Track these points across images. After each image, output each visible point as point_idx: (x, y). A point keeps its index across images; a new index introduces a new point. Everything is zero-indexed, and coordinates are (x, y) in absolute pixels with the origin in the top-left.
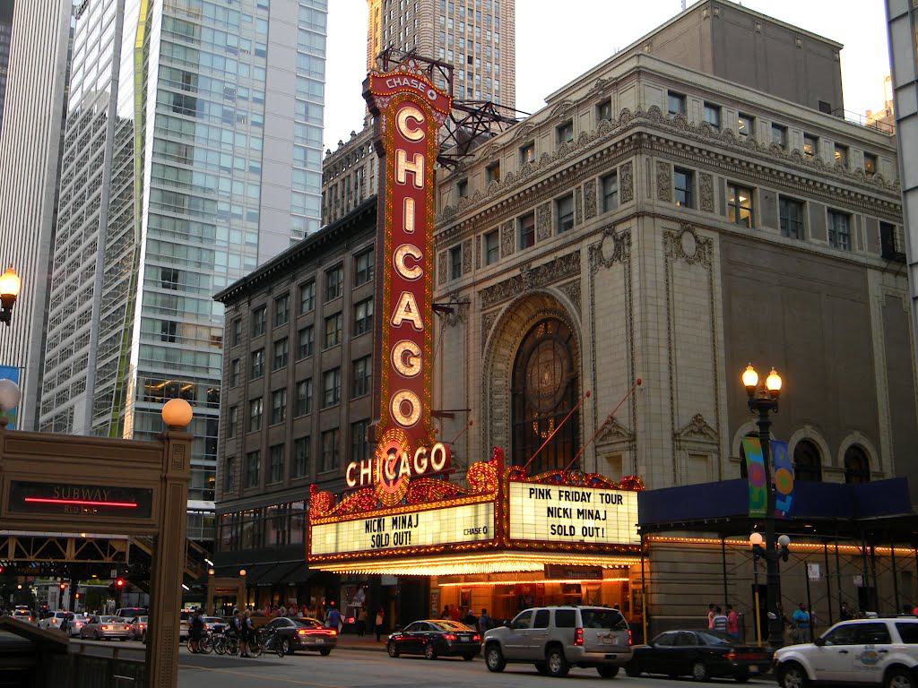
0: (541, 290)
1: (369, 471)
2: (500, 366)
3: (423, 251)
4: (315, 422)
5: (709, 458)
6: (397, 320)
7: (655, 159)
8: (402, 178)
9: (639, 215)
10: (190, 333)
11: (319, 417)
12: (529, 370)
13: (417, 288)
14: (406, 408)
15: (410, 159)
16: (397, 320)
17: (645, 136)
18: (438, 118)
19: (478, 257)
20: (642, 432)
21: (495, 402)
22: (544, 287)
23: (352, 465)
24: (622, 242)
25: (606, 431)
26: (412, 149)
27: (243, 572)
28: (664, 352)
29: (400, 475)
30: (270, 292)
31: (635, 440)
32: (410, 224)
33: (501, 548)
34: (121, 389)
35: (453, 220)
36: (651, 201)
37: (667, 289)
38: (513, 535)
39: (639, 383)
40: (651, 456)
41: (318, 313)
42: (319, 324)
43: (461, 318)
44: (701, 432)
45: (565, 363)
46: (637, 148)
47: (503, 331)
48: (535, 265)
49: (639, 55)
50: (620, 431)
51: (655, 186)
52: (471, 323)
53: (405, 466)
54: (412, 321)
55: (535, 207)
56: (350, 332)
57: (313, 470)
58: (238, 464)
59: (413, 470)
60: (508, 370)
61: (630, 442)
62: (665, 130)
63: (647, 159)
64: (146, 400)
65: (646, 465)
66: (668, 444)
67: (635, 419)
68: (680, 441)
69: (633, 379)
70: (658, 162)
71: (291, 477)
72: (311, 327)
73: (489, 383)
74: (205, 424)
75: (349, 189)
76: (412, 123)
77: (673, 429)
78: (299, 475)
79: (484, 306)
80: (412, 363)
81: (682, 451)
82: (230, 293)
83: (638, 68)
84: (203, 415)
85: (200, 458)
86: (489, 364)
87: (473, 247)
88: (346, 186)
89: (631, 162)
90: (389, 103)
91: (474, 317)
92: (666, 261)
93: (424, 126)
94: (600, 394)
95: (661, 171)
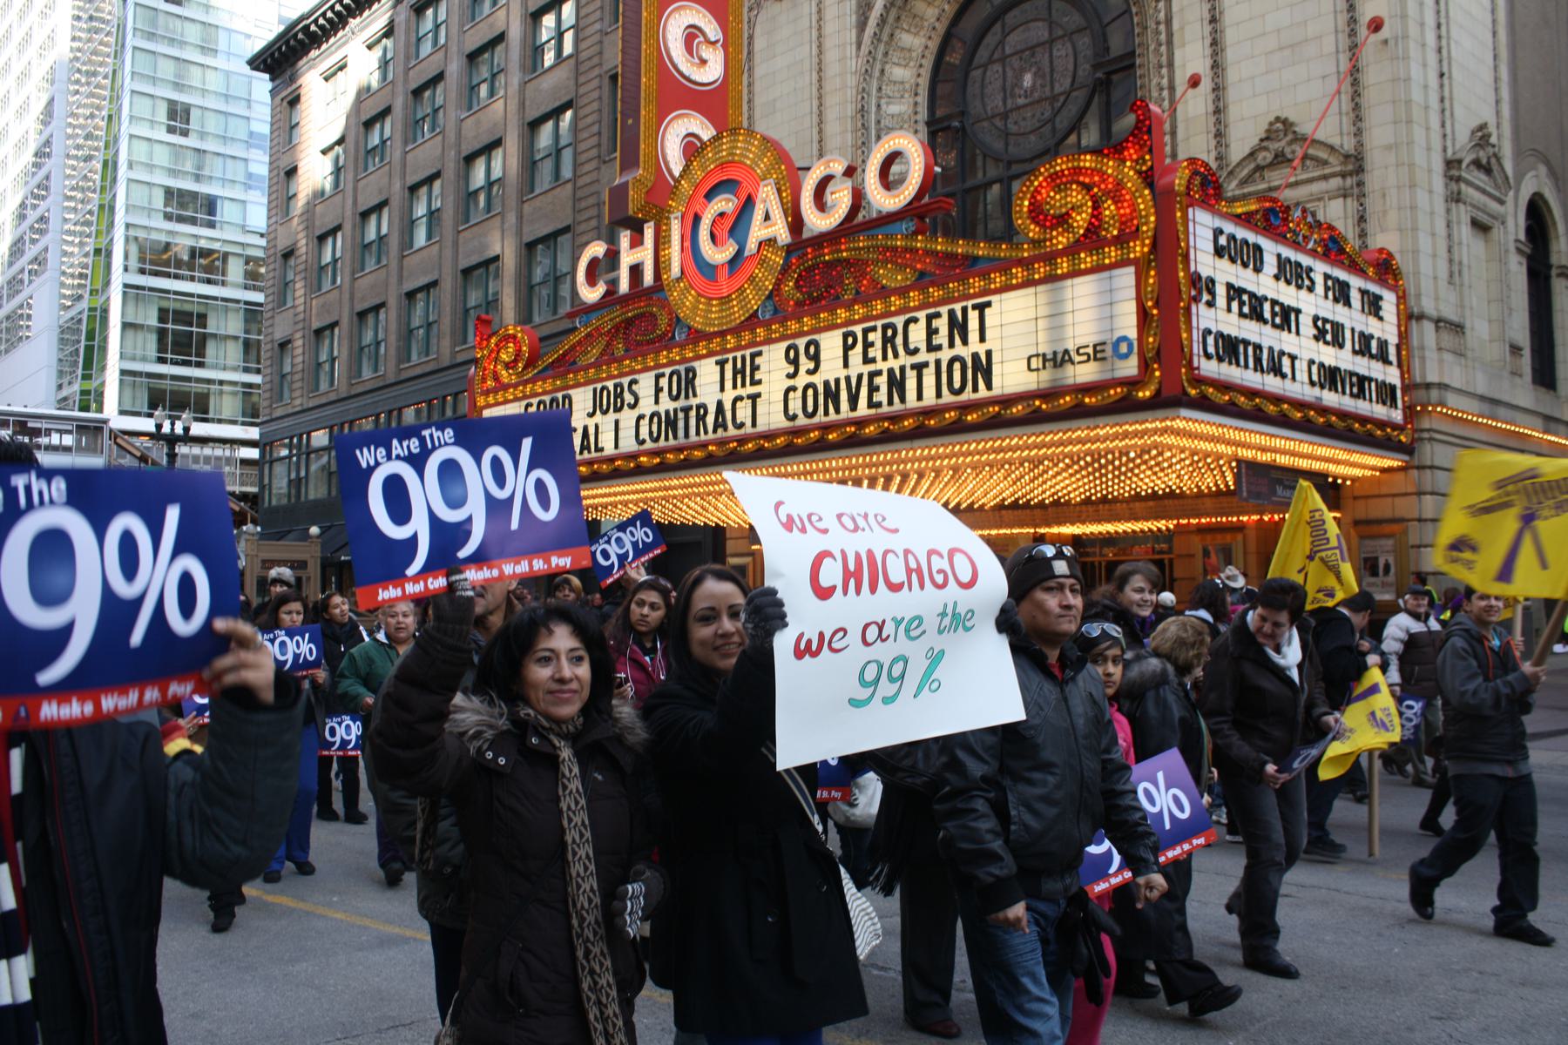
1: (645, 255)
2: (898, 73)
4: (448, 253)
5: (1495, 231)
10: (213, 124)
11: (456, 244)
12: (976, 74)
20: (1389, 148)
23: (597, 249)
25: (1265, 157)
27: (314, 530)
29: (751, 246)
31: (1360, 170)
33: (1166, 401)
39: (1376, 25)
41: (454, 48)
42: (454, 68)
44: (1488, 170)
45: (1084, 41)
50: (1311, 151)
53: (767, 217)
56: (523, 68)
57: (446, 343)
58: (300, 351)
59: (796, 224)
60: (920, 80)
61: (1343, 175)
64: (142, 272)
65: (1400, 230)
66: (1438, 182)
67: (1359, 118)
68: (1459, 179)
69: (1353, 21)
71: (400, 361)
72: (439, 77)
73: (874, 109)
74: (242, 313)
77: (1445, 150)
78: (414, 357)
80: (705, 55)
81: (1462, 206)
82: (287, 42)
84: (238, 301)
85: (235, 369)
86: (872, 71)
94: (1232, 75)
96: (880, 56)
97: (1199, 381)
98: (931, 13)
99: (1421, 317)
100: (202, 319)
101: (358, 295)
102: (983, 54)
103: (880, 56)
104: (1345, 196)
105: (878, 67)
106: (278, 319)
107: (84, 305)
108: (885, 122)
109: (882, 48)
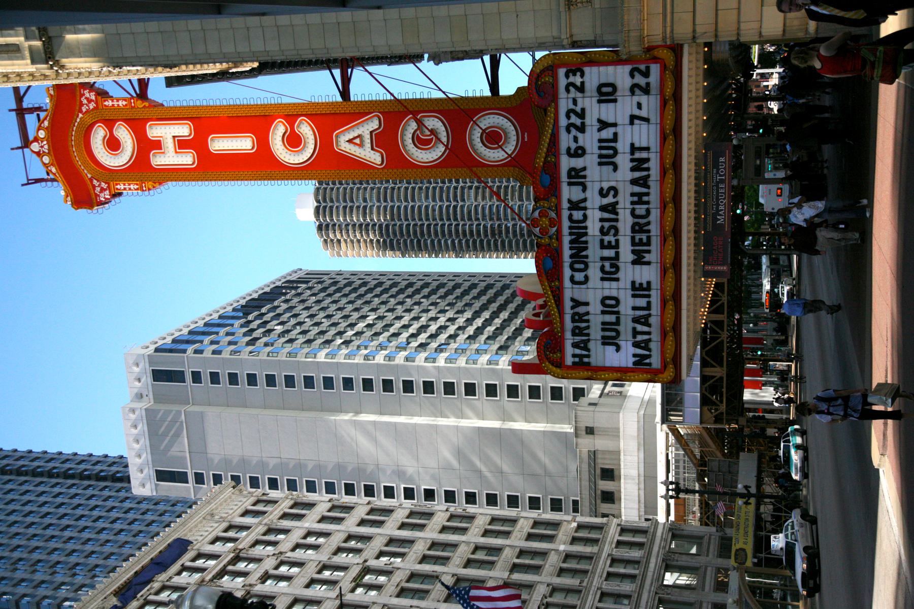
6: (375, 158)
8: (187, 159)
16: (375, 158)
18: (89, 101)
32: (243, 144)
54: (371, 132)
76: (113, 145)
93: (110, 124)
97: (665, 366)
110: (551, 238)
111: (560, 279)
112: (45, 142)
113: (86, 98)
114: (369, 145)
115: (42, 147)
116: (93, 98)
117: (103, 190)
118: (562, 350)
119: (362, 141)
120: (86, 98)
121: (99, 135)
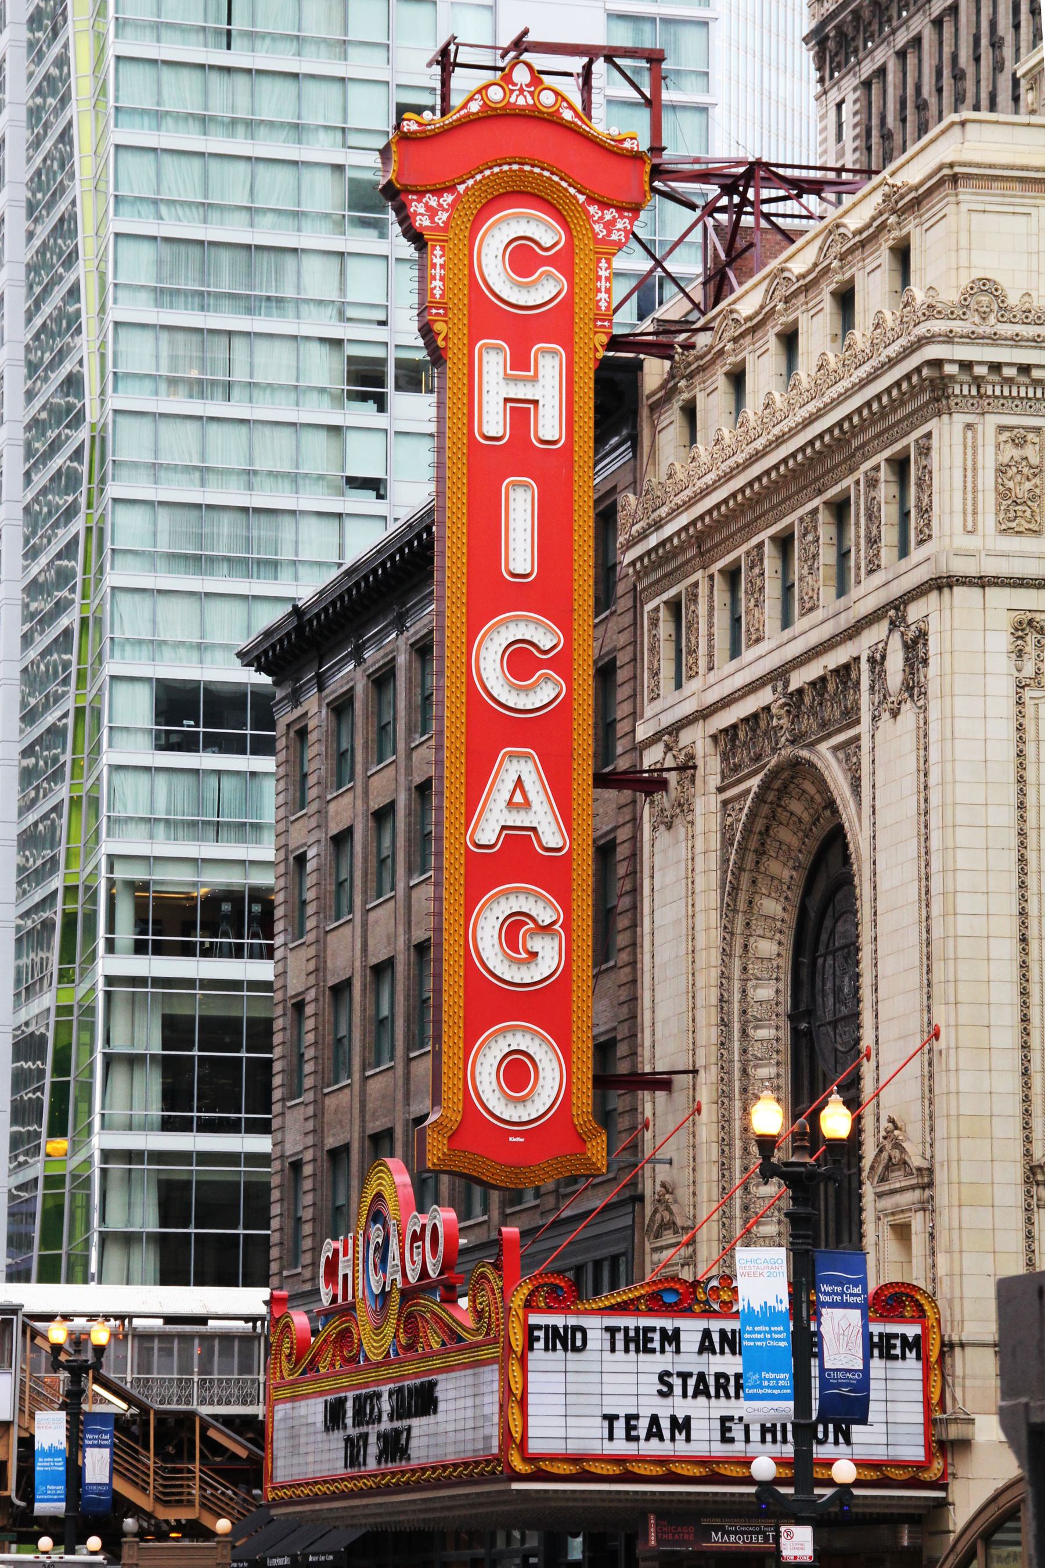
0: (805, 753)
3: (564, 622)
7: (992, 421)
8: (494, 422)
9: (942, 583)
12: (820, 961)
13: (542, 733)
14: (517, 1073)
15: (520, 362)
16: (487, 832)
17: (950, 369)
18: (609, 225)
19: (710, 636)
21: (756, 1050)
22: (812, 745)
24: (916, 648)
26: (522, 333)
28: (1007, 949)
30: (400, 625)
31: (930, 1185)
32: (520, 555)
34: (79, 907)
35: (658, 525)
36: (971, 543)
37: (1021, 780)
38: (535, 1447)
40: (960, 1228)
43: (684, 806)
46: (938, 400)
47: (761, 852)
48: (799, 679)
49: (963, 123)
51: (988, 500)
52: (699, 827)
54: (534, 829)
55: (793, 518)
61: (923, 1187)
62: (1016, 341)
63: (969, 426)
64: (140, 948)
70: (1002, 429)
73: (737, 996)
75: (993, 25)
76: (523, 258)
77: (1028, 1154)
79: (723, 777)
83: (951, 165)
87: (702, 608)
88: (947, 50)
89: (929, 435)
90: (452, 205)
91: (706, 805)
92: (1020, 703)
93: (564, 261)
95: (1010, 452)
96: (739, 928)
98: (786, 874)
99: (962, 1345)
100: (261, 1033)
101: (370, 1106)
102: (824, 937)
103: (739, 928)
104: (924, 1210)
105: (739, 942)
106: (289, 1116)
107: (46, 1000)
108: (753, 1011)
109: (740, 919)
110: (707, 1302)
111: (651, 1312)
112: (531, 102)
113: (612, 223)
114: (510, 823)
115: (521, 91)
116: (614, 237)
117: (432, 212)
118: (549, 1310)
119: (518, 807)
120: (612, 223)
121: (545, 232)
